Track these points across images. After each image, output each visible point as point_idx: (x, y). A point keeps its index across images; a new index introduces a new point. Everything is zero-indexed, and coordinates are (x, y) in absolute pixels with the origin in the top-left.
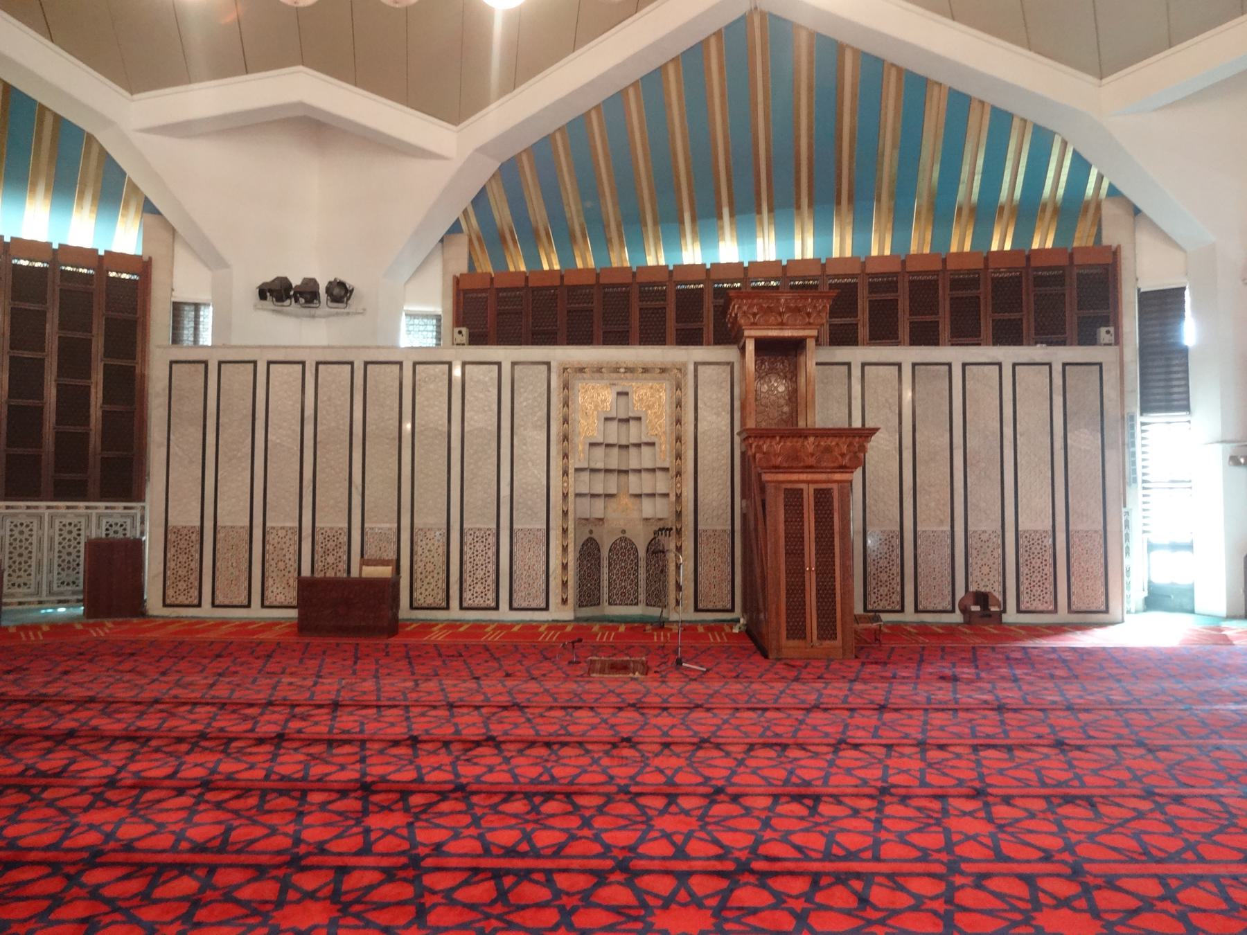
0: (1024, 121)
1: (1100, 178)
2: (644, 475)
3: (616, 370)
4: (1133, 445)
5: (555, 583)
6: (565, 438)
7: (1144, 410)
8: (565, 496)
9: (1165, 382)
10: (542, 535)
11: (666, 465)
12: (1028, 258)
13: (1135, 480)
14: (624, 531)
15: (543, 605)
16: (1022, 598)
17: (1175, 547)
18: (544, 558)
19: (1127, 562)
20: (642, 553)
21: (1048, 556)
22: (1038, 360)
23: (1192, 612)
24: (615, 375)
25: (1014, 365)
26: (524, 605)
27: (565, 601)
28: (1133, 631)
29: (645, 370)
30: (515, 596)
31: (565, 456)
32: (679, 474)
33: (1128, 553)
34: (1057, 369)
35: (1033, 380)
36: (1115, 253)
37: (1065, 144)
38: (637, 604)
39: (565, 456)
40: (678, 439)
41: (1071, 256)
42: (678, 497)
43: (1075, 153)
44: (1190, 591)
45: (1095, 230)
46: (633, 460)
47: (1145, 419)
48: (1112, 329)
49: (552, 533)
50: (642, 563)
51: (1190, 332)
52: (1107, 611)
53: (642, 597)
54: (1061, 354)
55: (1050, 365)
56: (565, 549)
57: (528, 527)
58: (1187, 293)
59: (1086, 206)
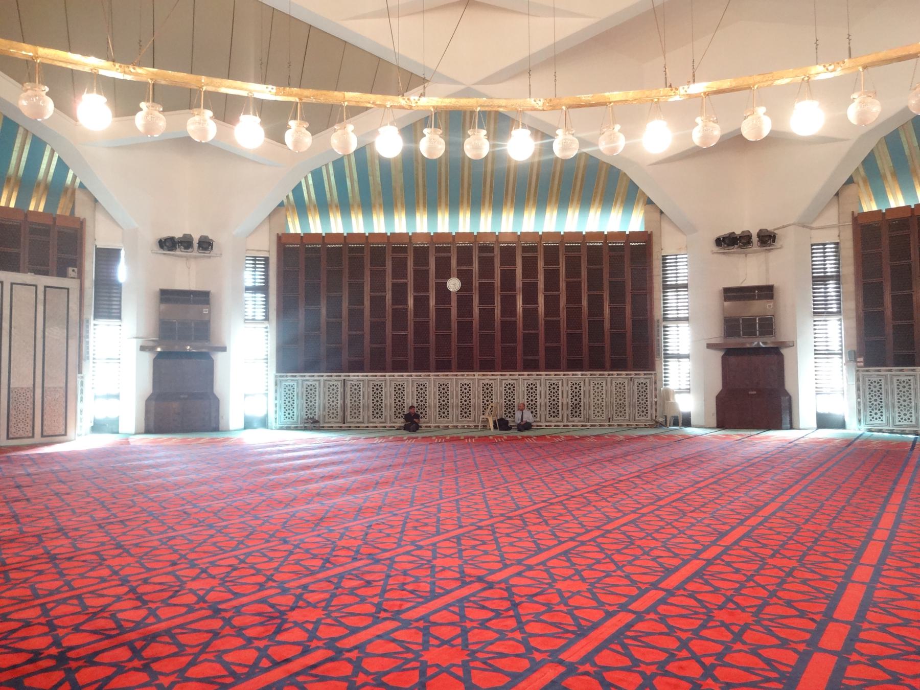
0: (27, 131)
1: (75, 177)
4: (88, 337)
7: (96, 317)
9: (107, 301)
12: (26, 215)
13: (88, 358)
16: (11, 430)
17: (109, 396)
19: (80, 406)
21: (29, 404)
22: (28, 282)
23: (118, 433)
25: (12, 284)
28: (80, 440)
33: (81, 401)
34: (41, 290)
35: (24, 296)
36: (82, 223)
37: (53, 152)
41: (54, 219)
43: (59, 158)
44: (116, 422)
45: (71, 206)
47: (96, 322)
48: (76, 269)
51: (122, 272)
52: (65, 435)
54: (44, 281)
55: (36, 286)
58: (123, 253)
59: (66, 190)
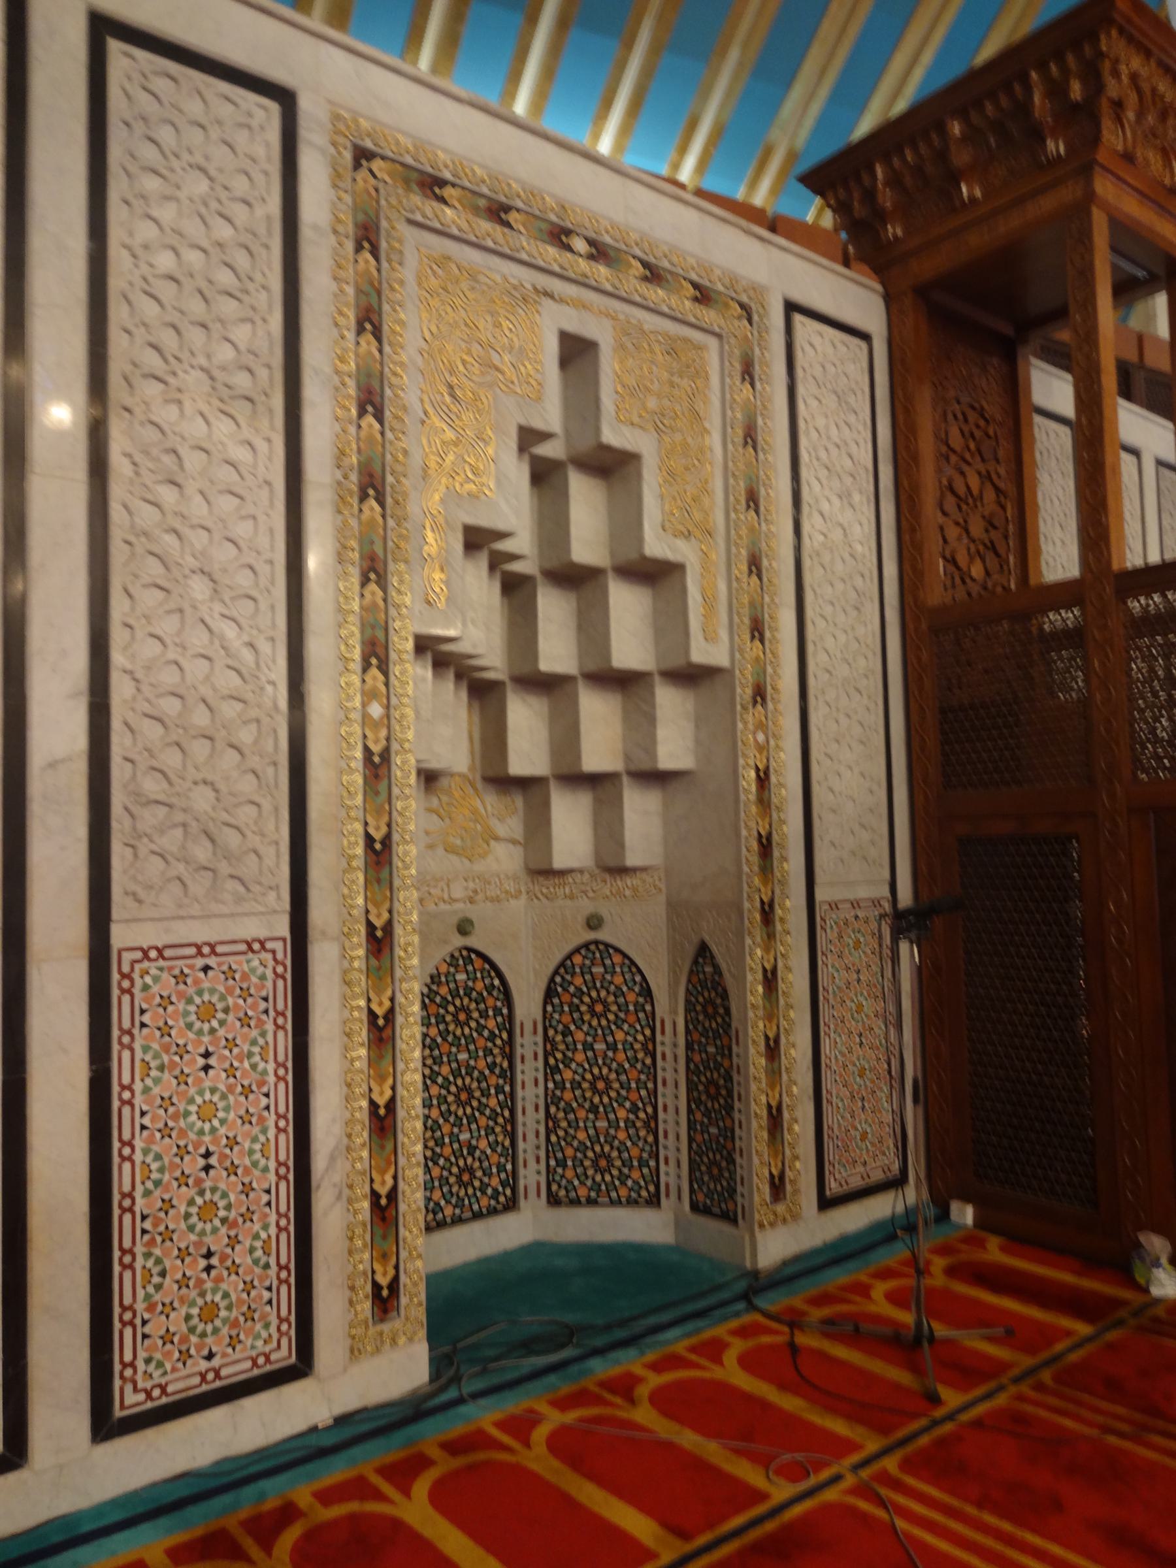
3: (559, 236)
5: (336, 1219)
6: (372, 484)
8: (377, 766)
10: (267, 974)
14: (464, 927)
15: (284, 1355)
18: (283, 1098)
20: (528, 1004)
24: (551, 254)
26: (184, 1381)
27: (385, 1300)
29: (653, 274)
30: (125, 1344)
31: (374, 570)
32: (759, 694)
38: (511, 1205)
39: (374, 570)
49: (324, 959)
50: (528, 1044)
53: (531, 1175)
56: (381, 1030)
57: (201, 933)
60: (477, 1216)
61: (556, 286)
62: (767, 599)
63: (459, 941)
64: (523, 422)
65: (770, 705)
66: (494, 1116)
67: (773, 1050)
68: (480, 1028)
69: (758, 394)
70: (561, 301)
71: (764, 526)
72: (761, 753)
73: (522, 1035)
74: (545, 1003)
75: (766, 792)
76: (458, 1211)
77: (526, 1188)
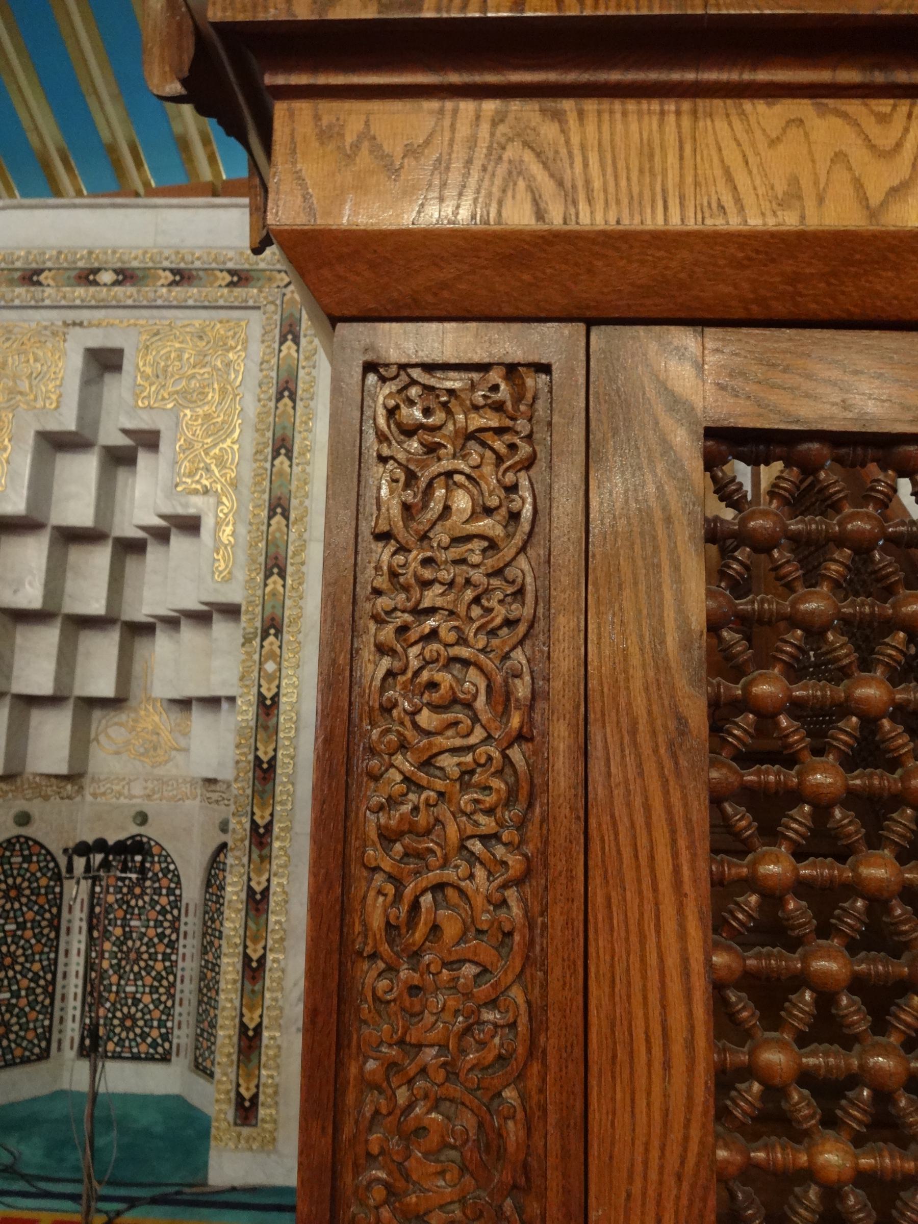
2: (188, 633)
3: (87, 277)
11: (234, 594)
14: (142, 818)
29: (182, 276)
32: (273, 626)
38: (165, 1058)
40: (279, 506)
42: (268, 707)
46: (162, 584)
60: (136, 1058)
61: (85, 315)
62: (293, 536)
63: (134, 830)
64: (40, 428)
65: (287, 637)
66: (159, 978)
67: (253, 970)
68: (154, 903)
69: (301, 349)
70: (90, 325)
71: (296, 470)
72: (270, 681)
73: (186, 915)
74: (207, 892)
75: (275, 719)
76: (118, 1049)
77: (178, 1045)
